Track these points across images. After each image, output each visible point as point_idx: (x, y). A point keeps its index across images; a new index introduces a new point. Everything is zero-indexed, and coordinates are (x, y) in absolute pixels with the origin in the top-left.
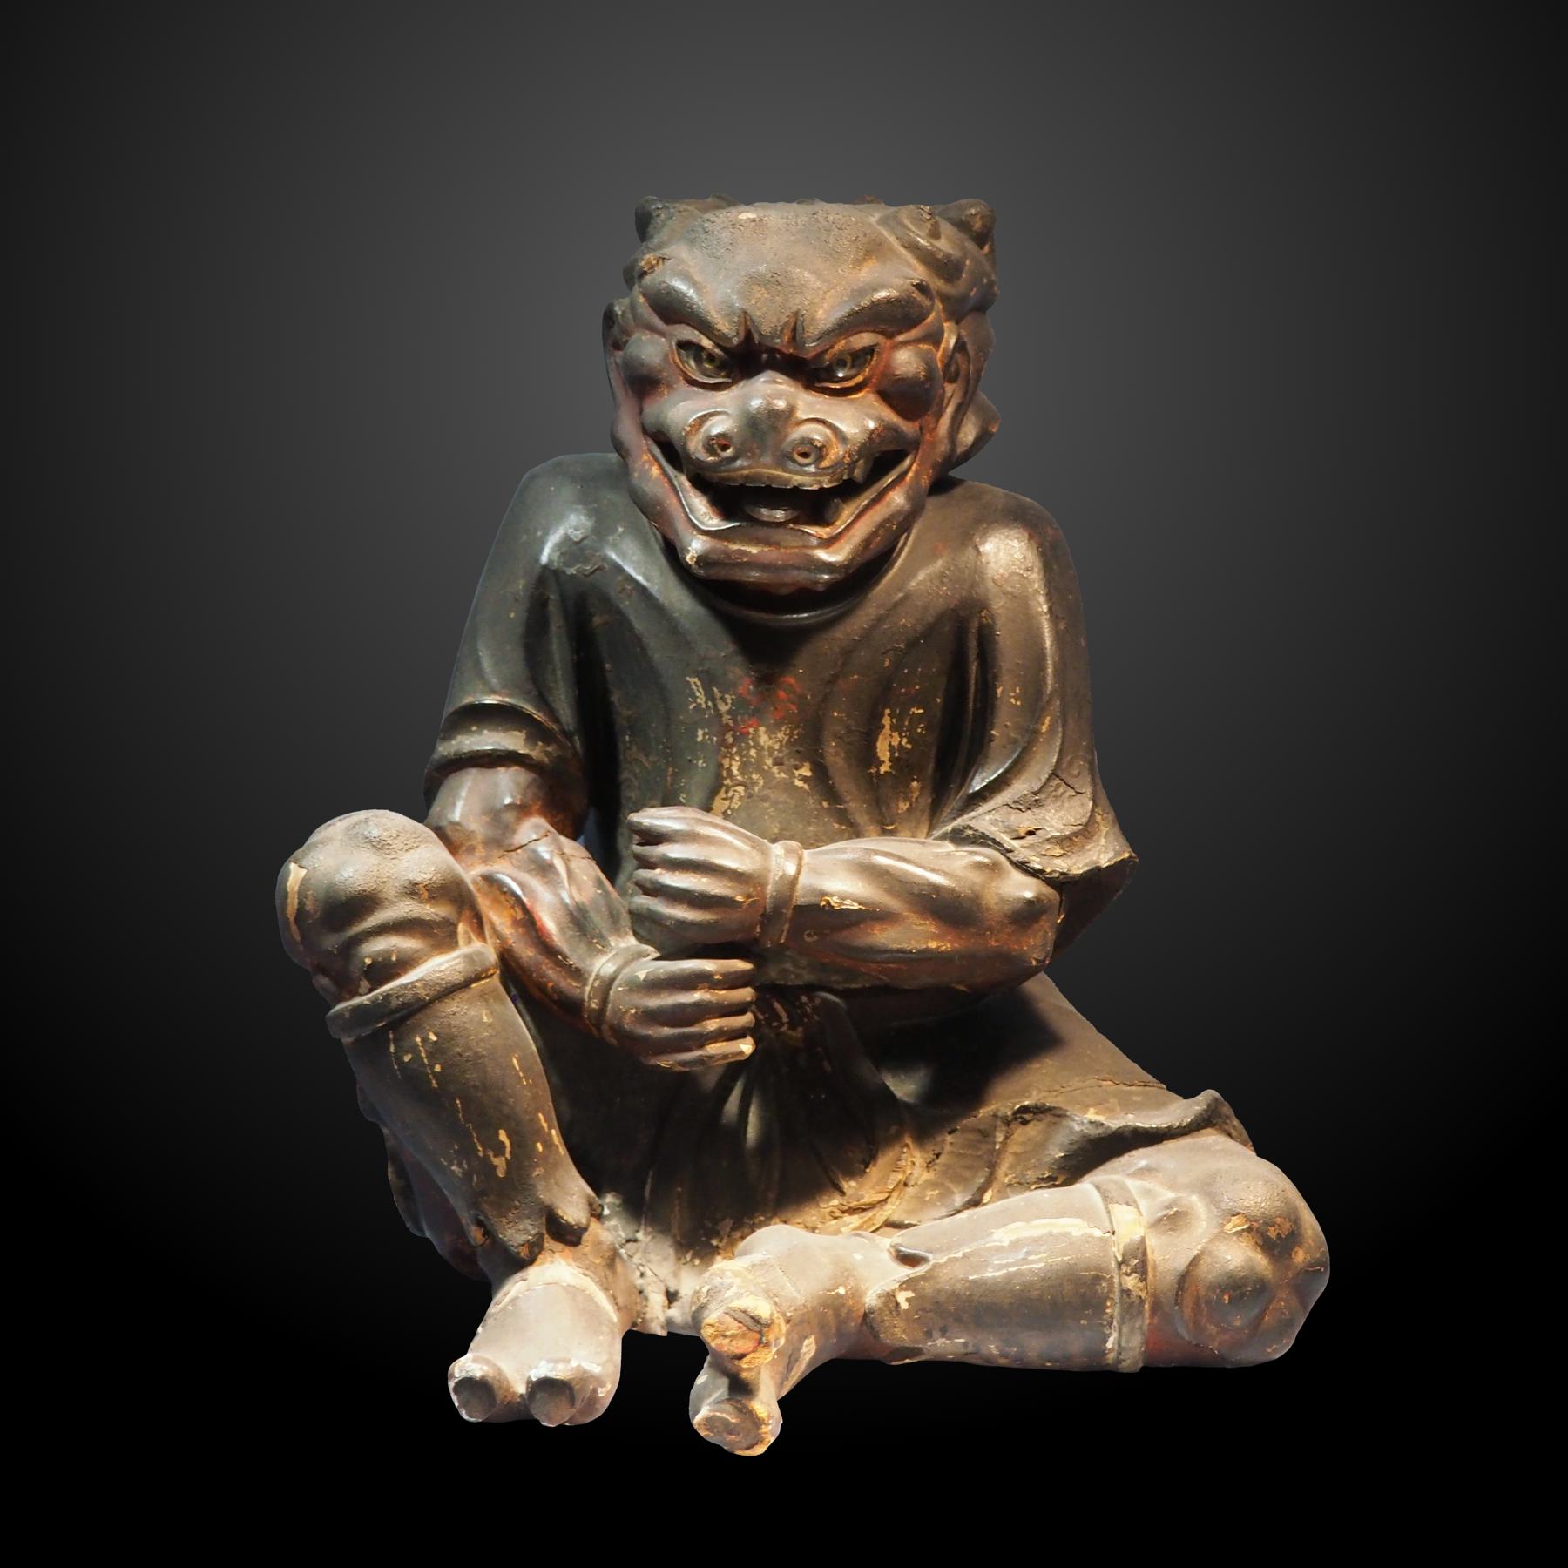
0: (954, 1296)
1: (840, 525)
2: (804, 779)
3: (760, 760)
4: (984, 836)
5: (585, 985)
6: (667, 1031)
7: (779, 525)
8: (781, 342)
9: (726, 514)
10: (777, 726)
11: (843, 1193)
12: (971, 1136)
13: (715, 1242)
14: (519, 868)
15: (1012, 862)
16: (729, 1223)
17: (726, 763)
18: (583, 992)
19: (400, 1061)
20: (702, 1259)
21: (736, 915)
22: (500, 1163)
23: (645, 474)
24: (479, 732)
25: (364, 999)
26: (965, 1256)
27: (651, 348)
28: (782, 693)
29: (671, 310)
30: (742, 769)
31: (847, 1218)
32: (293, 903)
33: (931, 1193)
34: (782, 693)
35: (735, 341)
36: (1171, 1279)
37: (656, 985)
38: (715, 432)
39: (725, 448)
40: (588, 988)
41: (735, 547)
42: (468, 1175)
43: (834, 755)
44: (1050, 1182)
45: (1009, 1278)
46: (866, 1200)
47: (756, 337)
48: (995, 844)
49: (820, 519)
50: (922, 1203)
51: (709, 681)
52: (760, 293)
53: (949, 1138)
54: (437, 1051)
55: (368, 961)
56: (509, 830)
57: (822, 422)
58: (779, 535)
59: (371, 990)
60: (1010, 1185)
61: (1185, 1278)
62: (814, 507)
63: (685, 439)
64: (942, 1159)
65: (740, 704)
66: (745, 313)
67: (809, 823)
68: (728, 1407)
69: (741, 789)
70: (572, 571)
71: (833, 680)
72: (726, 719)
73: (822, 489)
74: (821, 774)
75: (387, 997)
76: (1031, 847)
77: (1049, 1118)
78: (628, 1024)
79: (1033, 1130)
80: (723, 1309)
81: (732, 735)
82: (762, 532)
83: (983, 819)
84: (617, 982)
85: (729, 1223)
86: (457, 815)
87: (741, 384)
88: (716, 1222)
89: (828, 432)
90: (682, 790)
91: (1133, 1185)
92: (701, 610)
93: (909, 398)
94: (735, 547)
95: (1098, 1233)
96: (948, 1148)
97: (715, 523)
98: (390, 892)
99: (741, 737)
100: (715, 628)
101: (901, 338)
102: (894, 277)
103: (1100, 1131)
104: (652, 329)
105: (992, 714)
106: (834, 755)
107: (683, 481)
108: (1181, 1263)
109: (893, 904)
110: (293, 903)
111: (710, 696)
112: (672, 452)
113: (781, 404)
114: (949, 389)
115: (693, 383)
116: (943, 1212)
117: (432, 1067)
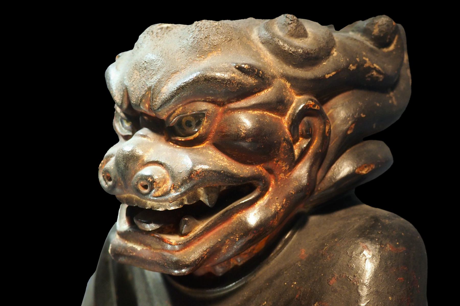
1: (191, 235)
8: (144, 108)
41: (130, 245)
49: (176, 231)
52: (136, 75)
58: (149, 240)
62: (171, 222)
73: (166, 211)
82: (141, 237)
89: (164, 171)
93: (261, 148)
101: (233, 105)
102: (222, 64)
113: (139, 152)
114: (303, 143)
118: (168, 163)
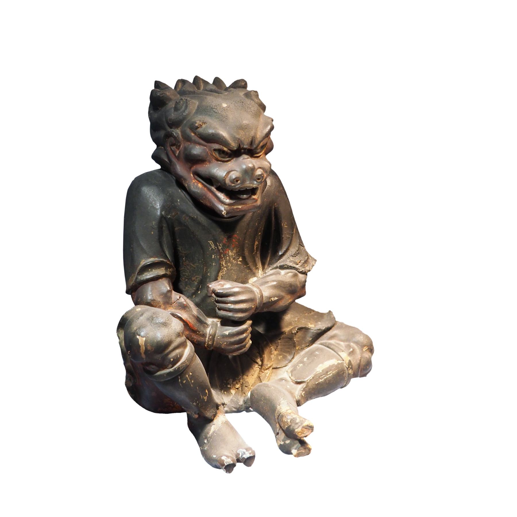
0: (313, 389)
2: (240, 261)
3: (230, 260)
4: (291, 267)
5: (206, 337)
6: (236, 346)
7: (245, 199)
9: (231, 198)
10: (233, 249)
11: (257, 363)
12: (286, 340)
13: (229, 386)
14: (176, 309)
15: (299, 272)
16: (231, 380)
17: (222, 263)
18: (205, 340)
19: (182, 382)
20: (227, 392)
21: (252, 311)
22: (206, 398)
23: (197, 187)
24: (152, 271)
25: (171, 370)
26: (313, 378)
27: (197, 150)
28: (234, 240)
29: (210, 139)
30: (226, 264)
31: (266, 371)
32: (143, 349)
33: (280, 357)
34: (234, 240)
35: (235, 149)
36: (357, 367)
37: (231, 335)
38: (234, 177)
39: (237, 181)
40: (207, 339)
41: (235, 207)
42: (197, 404)
43: (246, 253)
44: (309, 346)
45: (325, 380)
46: (269, 366)
47: (242, 146)
48: (294, 268)
50: (279, 361)
51: (215, 242)
52: (242, 133)
53: (279, 341)
54: (192, 377)
55: (172, 360)
56: (170, 298)
57: (260, 168)
59: (172, 367)
60: (299, 350)
61: (359, 366)
63: (225, 180)
64: (279, 347)
65: (224, 246)
66: (239, 139)
67: (243, 273)
68: (301, 448)
69: (225, 268)
70: (169, 216)
71: (245, 234)
72: (221, 251)
74: (244, 258)
75: (179, 368)
76: (301, 266)
77: (304, 330)
78: (223, 347)
79: (300, 334)
80: (301, 427)
81: (221, 255)
82: (243, 201)
83: (287, 260)
84: (216, 335)
85: (231, 380)
86: (150, 298)
87: (234, 159)
88: (227, 381)
90: (209, 272)
91: (332, 342)
92: (210, 221)
94: (235, 207)
95: (340, 362)
96: (280, 344)
97: (228, 201)
98: (173, 338)
99: (226, 254)
100: (214, 225)
103: (320, 331)
104: (200, 144)
105: (282, 232)
106: (246, 253)
107: (213, 189)
108: (358, 361)
109: (283, 294)
110: (143, 349)
111: (216, 245)
112: (210, 180)
113: (250, 165)
115: (217, 160)
116: (287, 362)
117: (191, 382)
118: (261, 166)
